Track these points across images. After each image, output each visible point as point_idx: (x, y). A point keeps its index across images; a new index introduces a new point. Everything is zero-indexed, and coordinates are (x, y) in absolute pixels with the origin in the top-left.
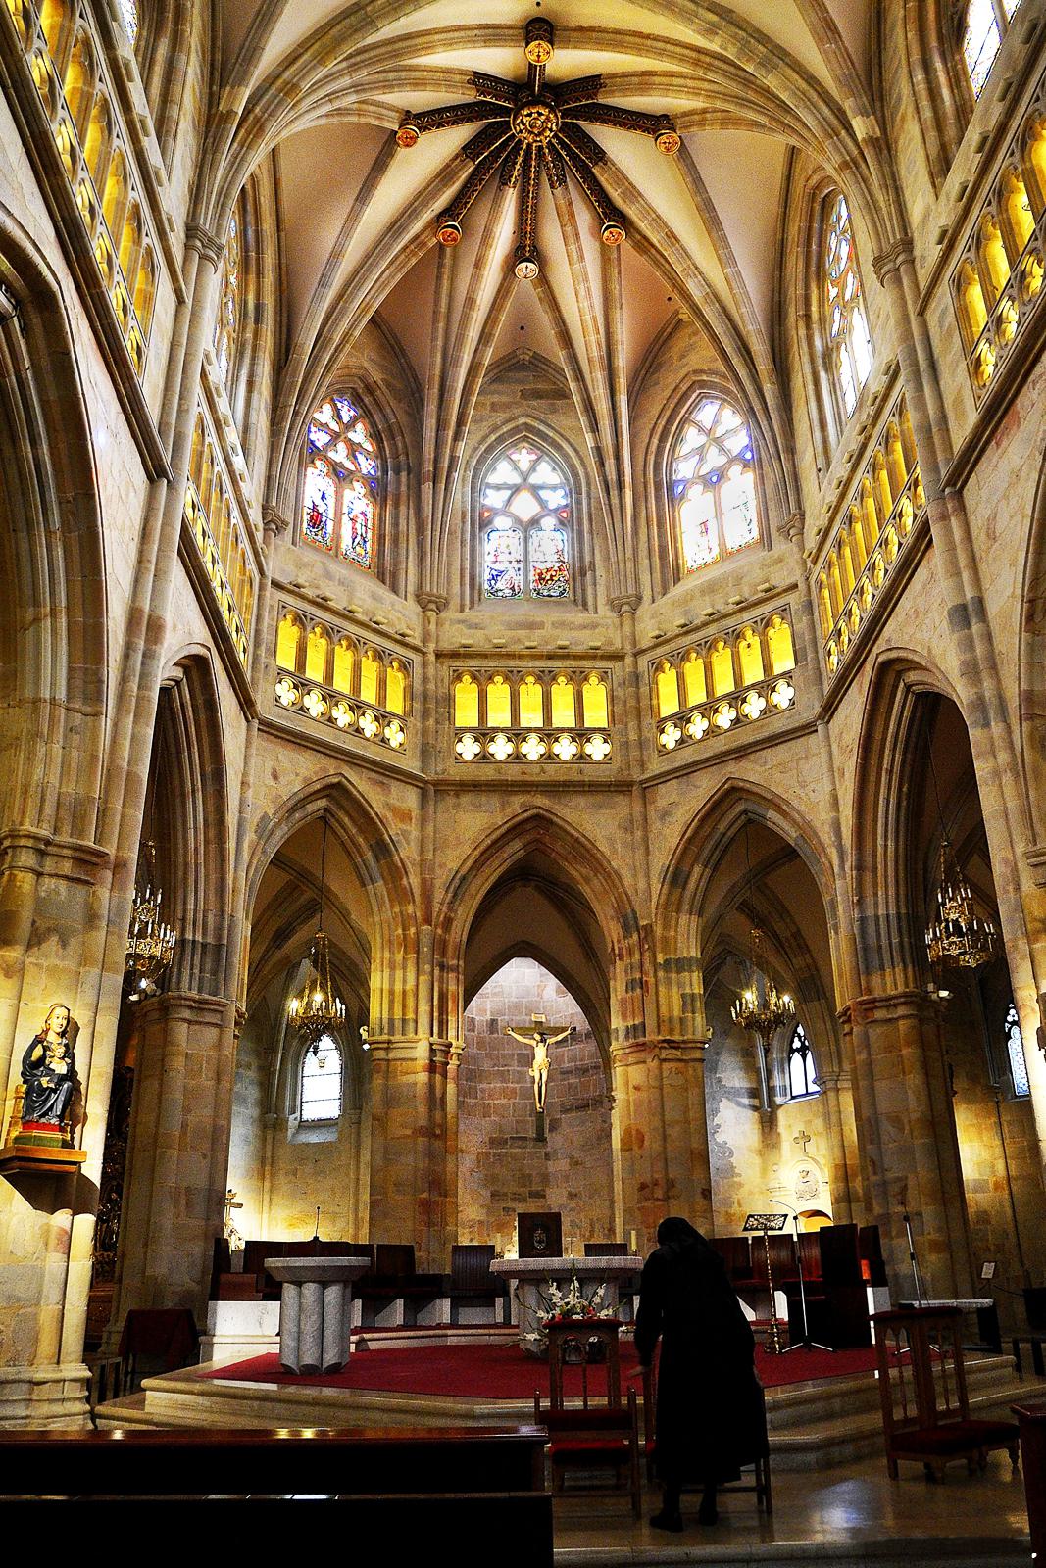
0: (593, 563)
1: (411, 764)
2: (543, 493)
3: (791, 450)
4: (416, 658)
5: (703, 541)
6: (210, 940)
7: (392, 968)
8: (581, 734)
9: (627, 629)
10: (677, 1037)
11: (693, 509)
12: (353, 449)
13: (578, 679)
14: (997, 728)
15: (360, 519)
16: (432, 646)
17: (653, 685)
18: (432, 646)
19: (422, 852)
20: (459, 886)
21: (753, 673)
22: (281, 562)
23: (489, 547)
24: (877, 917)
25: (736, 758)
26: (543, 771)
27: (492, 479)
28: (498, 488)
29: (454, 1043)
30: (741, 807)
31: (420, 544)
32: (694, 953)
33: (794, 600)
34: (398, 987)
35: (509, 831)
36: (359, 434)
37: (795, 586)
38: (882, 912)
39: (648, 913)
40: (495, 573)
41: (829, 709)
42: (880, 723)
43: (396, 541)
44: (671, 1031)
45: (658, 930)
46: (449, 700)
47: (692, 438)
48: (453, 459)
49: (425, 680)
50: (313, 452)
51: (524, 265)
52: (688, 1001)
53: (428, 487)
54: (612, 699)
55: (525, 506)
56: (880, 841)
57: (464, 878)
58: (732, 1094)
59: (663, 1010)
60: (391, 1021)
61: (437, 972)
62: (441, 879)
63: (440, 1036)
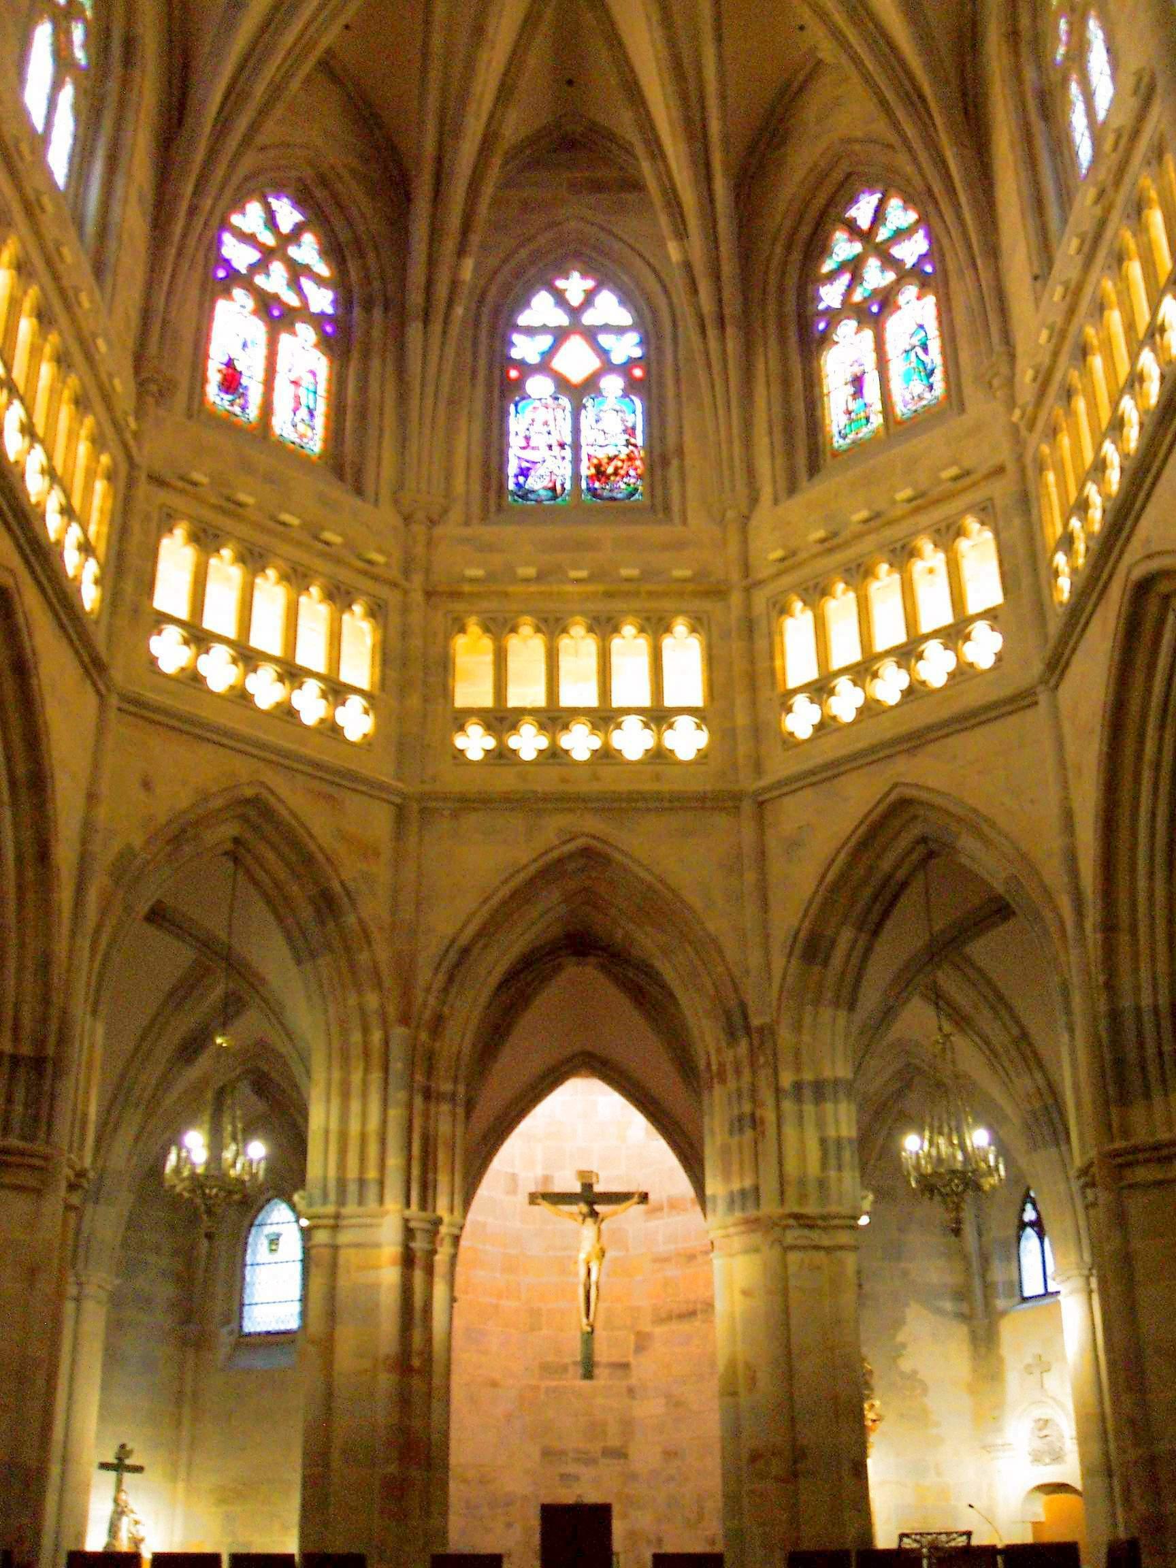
1: (382, 770)
2: (605, 340)
3: (993, 252)
4: (392, 597)
6: (26, 1049)
7: (345, 1095)
9: (733, 548)
10: (811, 1209)
12: (297, 272)
13: (656, 627)
15: (307, 380)
16: (418, 579)
17: (773, 638)
18: (418, 579)
19: (395, 908)
23: (517, 424)
24: (1138, 1009)
25: (907, 751)
26: (596, 778)
27: (523, 319)
28: (530, 331)
29: (446, 1218)
30: (916, 830)
31: (403, 420)
33: (1001, 491)
34: (354, 1127)
35: (543, 873)
36: (307, 251)
37: (1000, 470)
38: (1146, 1001)
40: (525, 465)
41: (1057, 665)
42: (1139, 677)
43: (362, 415)
44: (803, 1198)
45: (785, 1035)
46: (445, 665)
47: (843, 248)
48: (455, 284)
49: (405, 634)
53: (414, 331)
54: (711, 660)
56: (1142, 884)
57: (466, 951)
58: (927, 1297)
59: (791, 1167)
60: (342, 1183)
61: (418, 1101)
62: (429, 952)
63: (423, 1206)
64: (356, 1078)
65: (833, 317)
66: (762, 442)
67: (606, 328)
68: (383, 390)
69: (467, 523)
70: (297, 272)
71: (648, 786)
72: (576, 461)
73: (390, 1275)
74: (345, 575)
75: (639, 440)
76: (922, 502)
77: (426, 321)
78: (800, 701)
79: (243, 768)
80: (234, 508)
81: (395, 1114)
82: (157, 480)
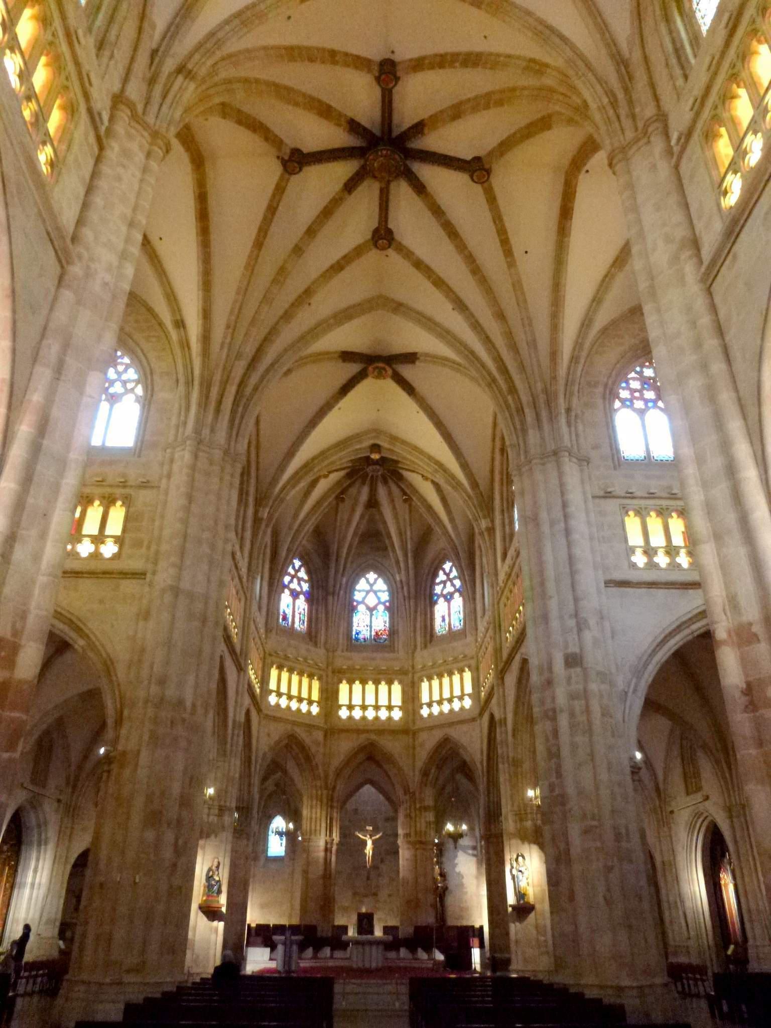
0: (398, 630)
2: (379, 594)
5: (443, 624)
6: (245, 805)
7: (312, 807)
8: (390, 708)
10: (423, 839)
11: (440, 608)
12: (300, 580)
13: (390, 683)
17: (419, 688)
18: (330, 668)
20: (338, 773)
22: (271, 645)
33: (473, 663)
34: (314, 816)
37: (472, 658)
39: (413, 786)
43: (316, 624)
45: (417, 794)
46: (336, 692)
48: (341, 584)
49: (327, 683)
52: (428, 824)
53: (330, 598)
54: (404, 692)
55: (371, 601)
58: (464, 849)
59: (418, 829)
62: (332, 769)
64: (314, 802)
65: (439, 596)
66: (418, 633)
67: (380, 591)
68: (322, 616)
69: (343, 651)
70: (300, 580)
72: (371, 631)
73: (322, 854)
74: (313, 671)
75: (387, 625)
76: (456, 660)
78: (425, 707)
79: (289, 727)
80: (286, 658)
81: (324, 813)
82: (270, 655)
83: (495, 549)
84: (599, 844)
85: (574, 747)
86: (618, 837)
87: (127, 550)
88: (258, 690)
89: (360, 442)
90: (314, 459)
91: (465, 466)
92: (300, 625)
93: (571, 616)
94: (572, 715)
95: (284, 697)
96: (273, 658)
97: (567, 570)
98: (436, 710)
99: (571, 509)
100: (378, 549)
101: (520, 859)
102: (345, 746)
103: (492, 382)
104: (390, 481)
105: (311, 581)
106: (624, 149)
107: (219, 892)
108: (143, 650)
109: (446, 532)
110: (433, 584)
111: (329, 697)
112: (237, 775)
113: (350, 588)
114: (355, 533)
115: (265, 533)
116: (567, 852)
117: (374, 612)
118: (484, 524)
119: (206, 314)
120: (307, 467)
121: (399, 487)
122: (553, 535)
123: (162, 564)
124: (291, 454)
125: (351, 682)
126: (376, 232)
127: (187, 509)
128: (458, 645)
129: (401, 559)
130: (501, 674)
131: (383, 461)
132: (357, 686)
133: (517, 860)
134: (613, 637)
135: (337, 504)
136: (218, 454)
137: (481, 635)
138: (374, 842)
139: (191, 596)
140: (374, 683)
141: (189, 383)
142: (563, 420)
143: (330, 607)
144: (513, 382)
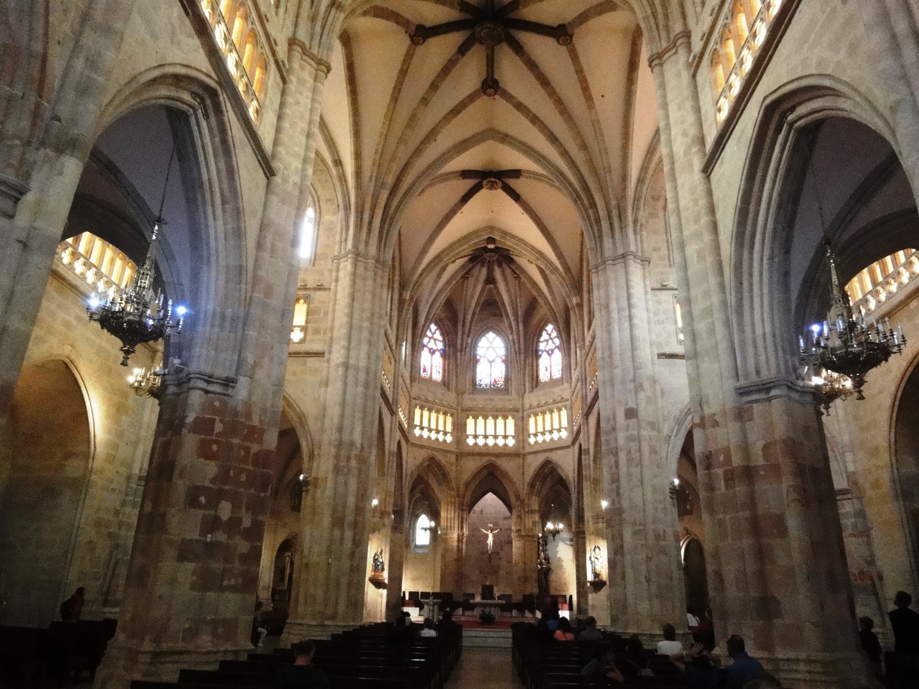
1: (453, 449)
7: (447, 510)
8: (505, 437)
10: (530, 534)
11: (544, 361)
13: (505, 418)
14: (589, 483)
17: (528, 421)
20: (468, 484)
21: (556, 426)
22: (415, 391)
32: (537, 508)
33: (568, 403)
37: (567, 400)
43: (449, 373)
45: (526, 501)
48: (467, 343)
49: (458, 419)
50: (424, 346)
51: (489, 286)
52: (534, 523)
53: (459, 354)
55: (491, 355)
58: (563, 540)
59: (527, 526)
62: (462, 483)
65: (543, 352)
66: (527, 379)
67: (497, 347)
70: (435, 340)
71: (503, 452)
74: (447, 410)
76: (555, 402)
77: (461, 351)
78: (532, 436)
80: (427, 401)
81: (456, 514)
82: (414, 399)
83: (583, 321)
84: (643, 542)
85: (629, 475)
86: (657, 537)
87: (309, 337)
88: (406, 426)
89: (478, 236)
90: (443, 252)
91: (560, 255)
92: (438, 377)
93: (631, 381)
94: (629, 452)
95: (426, 430)
96: (418, 402)
97: (630, 346)
98: (540, 439)
99: (634, 300)
100: (495, 315)
101: (597, 549)
102: (471, 466)
103: (577, 198)
104: (504, 265)
105: (444, 341)
106: (660, 56)
107: (383, 570)
108: (325, 408)
109: (547, 302)
110: (538, 341)
111: (459, 428)
112: (393, 490)
113: (474, 346)
114: (477, 304)
115: (408, 310)
116: (622, 547)
117: (493, 364)
118: (575, 300)
119: (358, 156)
120: (438, 258)
121: (510, 268)
122: (619, 319)
123: (335, 347)
124: (425, 250)
125: (476, 418)
126: (485, 82)
127: (351, 306)
128: (557, 390)
129: (513, 323)
130: (587, 415)
131: (497, 250)
132: (480, 420)
133: (594, 550)
134: (662, 396)
135: (463, 282)
136: (371, 262)
137: (573, 384)
138: (494, 536)
139: (357, 369)
140: (493, 418)
141: (347, 208)
142: (630, 230)
143: (459, 362)
144: (593, 198)
